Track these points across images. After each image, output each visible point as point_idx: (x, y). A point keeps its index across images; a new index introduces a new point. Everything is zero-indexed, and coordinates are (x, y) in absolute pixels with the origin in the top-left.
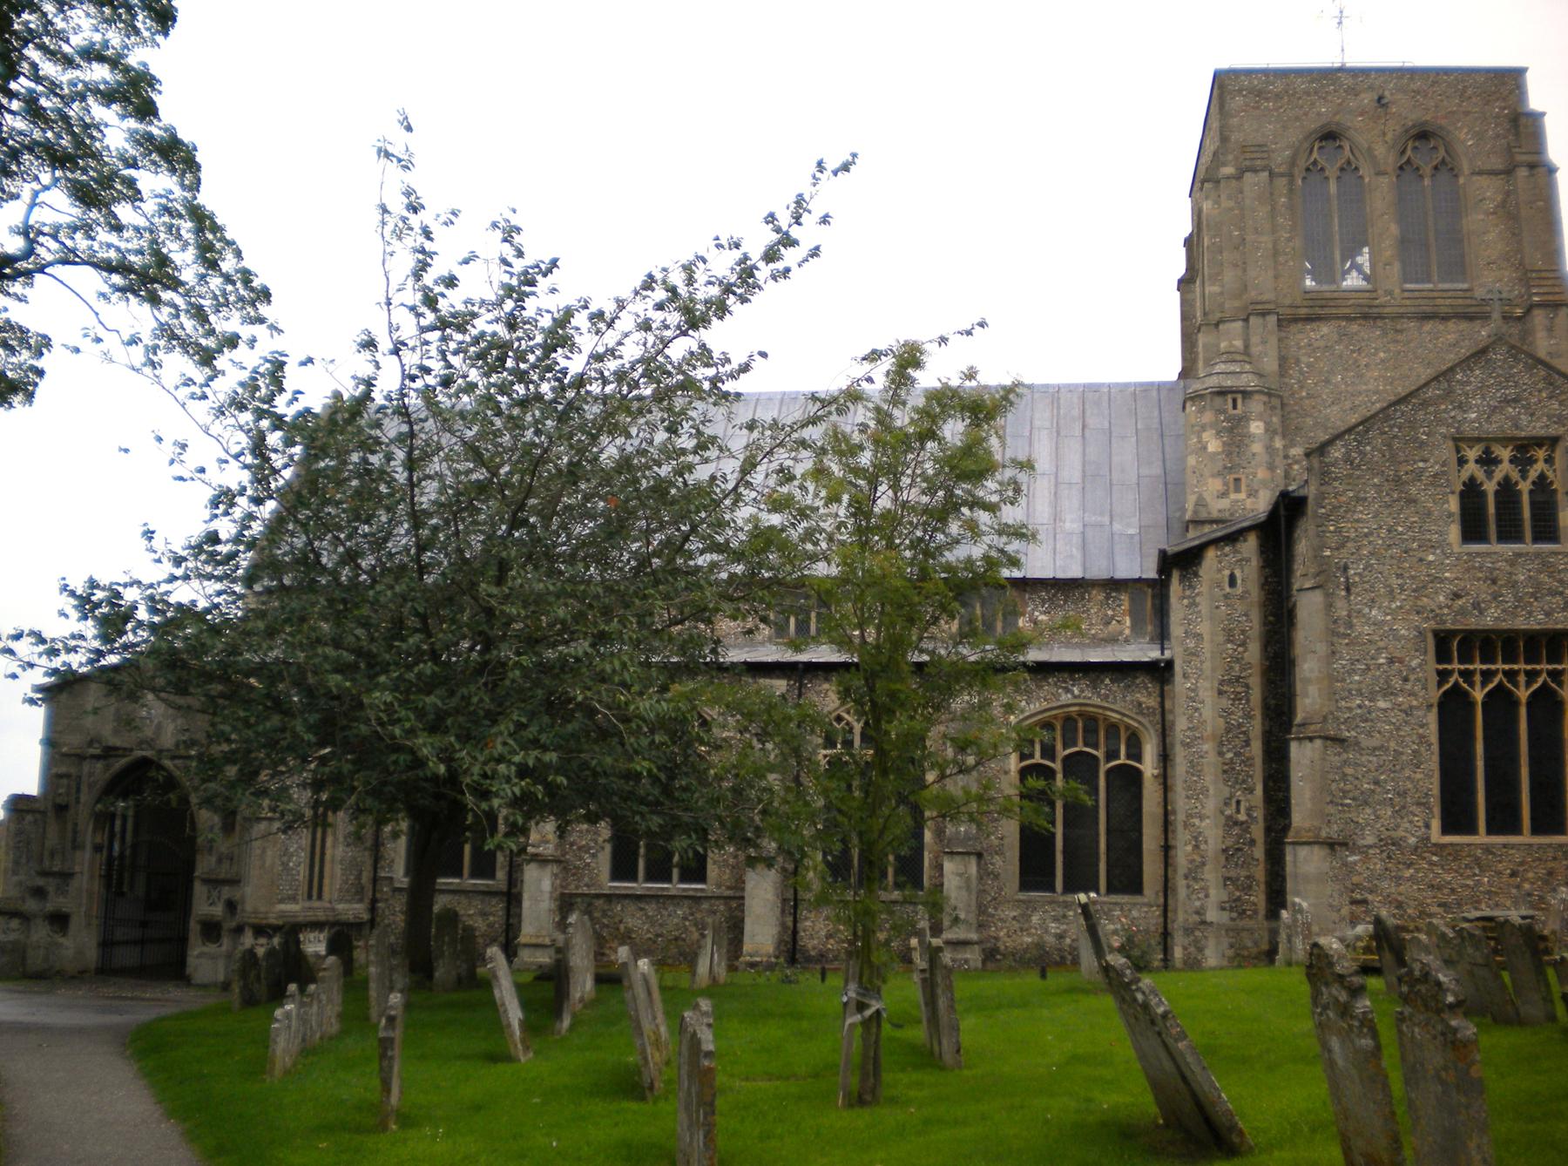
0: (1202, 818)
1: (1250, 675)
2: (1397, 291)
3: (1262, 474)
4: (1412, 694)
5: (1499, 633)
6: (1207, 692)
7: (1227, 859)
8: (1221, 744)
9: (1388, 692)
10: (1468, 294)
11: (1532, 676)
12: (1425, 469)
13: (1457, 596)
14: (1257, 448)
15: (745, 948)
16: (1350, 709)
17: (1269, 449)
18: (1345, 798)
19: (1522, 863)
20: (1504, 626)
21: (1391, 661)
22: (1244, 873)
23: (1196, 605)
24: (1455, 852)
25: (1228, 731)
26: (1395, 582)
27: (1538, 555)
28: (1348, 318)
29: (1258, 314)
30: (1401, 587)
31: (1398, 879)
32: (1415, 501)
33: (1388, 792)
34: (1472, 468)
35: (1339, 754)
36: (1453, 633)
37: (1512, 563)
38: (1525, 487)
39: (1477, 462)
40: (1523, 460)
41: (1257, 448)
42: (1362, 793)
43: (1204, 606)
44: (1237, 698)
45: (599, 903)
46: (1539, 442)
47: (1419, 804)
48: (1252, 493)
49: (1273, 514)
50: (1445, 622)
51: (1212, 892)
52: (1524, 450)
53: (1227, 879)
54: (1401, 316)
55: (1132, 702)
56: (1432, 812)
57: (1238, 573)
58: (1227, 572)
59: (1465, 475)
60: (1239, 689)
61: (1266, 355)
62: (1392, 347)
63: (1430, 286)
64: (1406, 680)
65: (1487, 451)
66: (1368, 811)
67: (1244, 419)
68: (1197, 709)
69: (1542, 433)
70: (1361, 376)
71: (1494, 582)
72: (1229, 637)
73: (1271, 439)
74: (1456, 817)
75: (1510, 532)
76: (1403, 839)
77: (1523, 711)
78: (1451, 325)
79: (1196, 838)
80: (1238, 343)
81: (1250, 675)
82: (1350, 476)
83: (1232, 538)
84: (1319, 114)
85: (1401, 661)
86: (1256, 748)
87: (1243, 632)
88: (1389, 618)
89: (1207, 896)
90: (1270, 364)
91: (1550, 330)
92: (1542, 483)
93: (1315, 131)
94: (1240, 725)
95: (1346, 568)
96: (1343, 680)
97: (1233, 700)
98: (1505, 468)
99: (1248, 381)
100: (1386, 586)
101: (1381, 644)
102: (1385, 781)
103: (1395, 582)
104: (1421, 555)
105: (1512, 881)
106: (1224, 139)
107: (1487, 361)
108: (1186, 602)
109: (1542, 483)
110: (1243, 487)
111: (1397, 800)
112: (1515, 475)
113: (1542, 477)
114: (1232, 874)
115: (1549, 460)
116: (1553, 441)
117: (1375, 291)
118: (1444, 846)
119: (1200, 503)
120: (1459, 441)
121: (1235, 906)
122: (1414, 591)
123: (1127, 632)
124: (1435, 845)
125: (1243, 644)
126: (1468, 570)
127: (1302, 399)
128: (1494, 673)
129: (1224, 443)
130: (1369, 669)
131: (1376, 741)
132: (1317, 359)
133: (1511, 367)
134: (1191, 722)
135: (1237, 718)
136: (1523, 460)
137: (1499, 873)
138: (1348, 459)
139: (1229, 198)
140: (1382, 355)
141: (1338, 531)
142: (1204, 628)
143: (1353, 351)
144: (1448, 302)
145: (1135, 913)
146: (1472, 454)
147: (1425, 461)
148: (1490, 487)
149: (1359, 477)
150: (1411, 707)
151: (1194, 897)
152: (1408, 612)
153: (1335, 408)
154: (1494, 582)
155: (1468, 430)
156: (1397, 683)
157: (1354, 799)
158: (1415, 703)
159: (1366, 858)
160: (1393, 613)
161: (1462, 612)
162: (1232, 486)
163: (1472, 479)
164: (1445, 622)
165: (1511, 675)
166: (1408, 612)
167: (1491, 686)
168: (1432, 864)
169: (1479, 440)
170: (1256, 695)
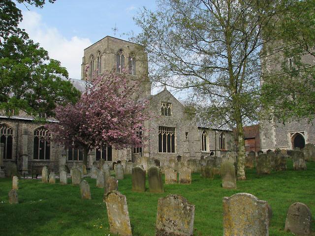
46: (169, 103)
74: (160, 151)
75: (166, 114)
120: (162, 102)
136: (167, 105)
146: (163, 104)
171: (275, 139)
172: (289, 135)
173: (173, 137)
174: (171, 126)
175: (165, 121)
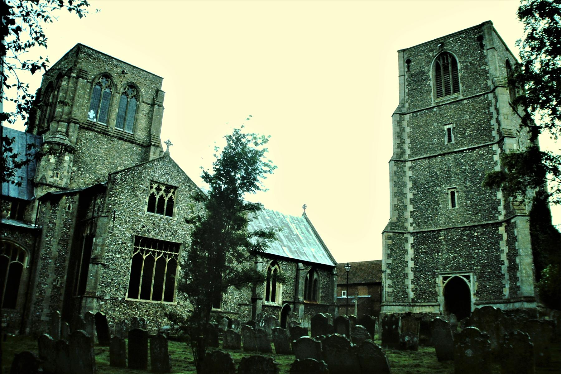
0: (45, 285)
1: (69, 239)
2: (114, 129)
3: (65, 173)
4: (126, 254)
7: (51, 299)
8: (56, 261)
9: (120, 252)
10: (133, 136)
11: (159, 254)
12: (141, 187)
13: (144, 227)
16: (108, 256)
18: (102, 283)
19: (149, 308)
20: (154, 238)
21: (122, 243)
22: (56, 304)
23: (56, 213)
24: (130, 304)
25: (59, 256)
26: (128, 219)
27: (167, 219)
28: (99, 132)
29: (73, 123)
30: (129, 221)
31: (114, 311)
32: (137, 196)
33: (115, 283)
34: (153, 190)
35: (103, 270)
36: (141, 237)
37: (160, 220)
38: (166, 199)
39: (155, 189)
40: (167, 191)
41: (66, 165)
42: (108, 282)
43: (58, 213)
44: (64, 246)
46: (172, 187)
47: (123, 288)
48: (61, 179)
50: (139, 234)
51: (45, 310)
52: (169, 188)
53: (50, 306)
54: (114, 136)
55: (24, 241)
56: (126, 290)
57: (71, 205)
58: (68, 204)
59: (151, 192)
60: (65, 243)
61: (73, 136)
62: (109, 145)
63: (123, 130)
64: (126, 249)
66: (108, 288)
68: (49, 248)
69: (174, 185)
70: (98, 151)
71: (154, 224)
73: (70, 163)
75: (160, 211)
76: (118, 298)
77: (155, 263)
78: (126, 143)
79: (41, 291)
80: (64, 130)
81: (69, 239)
82: (121, 184)
84: (105, 69)
85: (125, 243)
87: (69, 225)
88: (124, 230)
89: (42, 311)
90: (74, 139)
91: (154, 153)
92: (171, 199)
93: (102, 73)
94: (63, 255)
95: (115, 212)
96: (108, 247)
97: (62, 247)
98: (162, 192)
100: (125, 220)
101: (120, 237)
102: (115, 280)
103: (128, 219)
104: (136, 213)
105: (145, 313)
107: (163, 161)
108: (51, 211)
109: (171, 199)
110: (59, 176)
111: (117, 286)
112: (156, 193)
113: (171, 197)
114: (52, 304)
115: (174, 193)
116: (176, 188)
117: (107, 127)
118: (129, 301)
119: (44, 177)
120: (152, 181)
122: (132, 223)
123: (9, 215)
124: (126, 301)
125: (69, 229)
126: (148, 220)
127: (79, 153)
128: (161, 253)
129: (56, 161)
130: (116, 244)
131: (114, 267)
132: (86, 142)
133: (169, 164)
134: (46, 251)
135: (62, 253)
136: (167, 191)
137: (143, 311)
138: (121, 179)
139: (72, 83)
140: (105, 146)
141: (115, 200)
142: (57, 221)
143: (97, 143)
144: (127, 136)
145: (12, 315)
146: (155, 186)
147: (143, 185)
148: (158, 197)
149: (123, 185)
150: (126, 258)
151: (37, 311)
152: (129, 229)
153: (88, 158)
154: (154, 224)
156: (123, 250)
157: (105, 284)
158: (127, 257)
159: (106, 303)
160: (126, 228)
161: (144, 232)
162: (55, 175)
163: (153, 193)
164: (139, 234)
165: (154, 252)
166: (129, 229)
167: (148, 255)
168: (124, 306)
169: (157, 182)
170: (70, 245)
171: (411, 286)
172: (439, 280)
174: (170, 239)
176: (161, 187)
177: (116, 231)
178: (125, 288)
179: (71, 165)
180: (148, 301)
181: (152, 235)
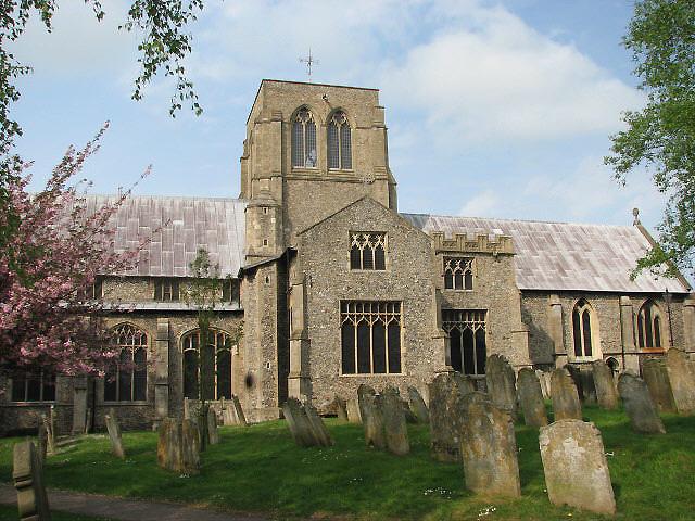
5: (363, 301)
6: (257, 322)
9: (325, 323)
14: (273, 228)
15: (75, 425)
17: (278, 229)
27: (378, 274)
40: (373, 238)
45: (8, 410)
49: (283, 256)
52: (374, 236)
65: (361, 236)
67: (269, 216)
72: (266, 301)
74: (348, 367)
75: (368, 265)
78: (345, 184)
83: (268, 264)
86: (275, 343)
99: (270, 202)
106: (265, 107)
120: (351, 233)
121: (267, 402)
136: (373, 238)
155: (354, 229)
161: (351, 293)
173: (394, 327)
175: (367, 284)
176: (365, 236)
177: (317, 300)
178: (337, 363)
179: (281, 227)
180: (367, 375)
181: (361, 296)
